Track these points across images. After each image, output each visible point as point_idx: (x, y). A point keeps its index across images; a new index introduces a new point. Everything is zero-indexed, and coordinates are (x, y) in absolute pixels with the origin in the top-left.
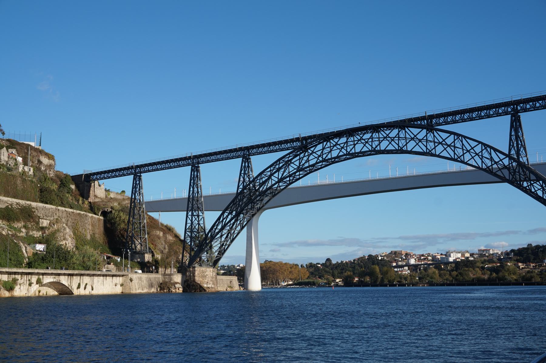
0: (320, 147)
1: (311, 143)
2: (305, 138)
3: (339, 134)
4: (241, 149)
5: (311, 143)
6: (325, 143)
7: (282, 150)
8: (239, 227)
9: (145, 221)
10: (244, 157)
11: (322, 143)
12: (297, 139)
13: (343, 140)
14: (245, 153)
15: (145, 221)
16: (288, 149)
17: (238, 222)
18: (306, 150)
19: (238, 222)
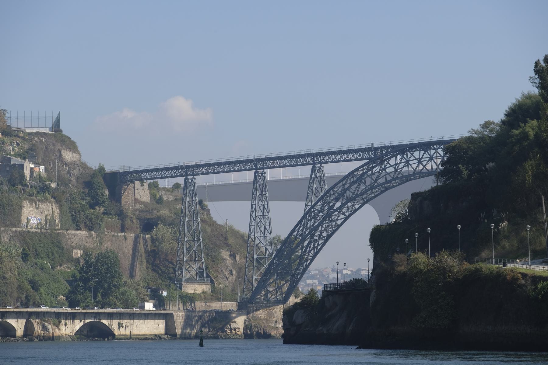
0: (392, 161)
1: (386, 155)
2: (381, 148)
3: (413, 147)
4: (309, 155)
5: (386, 155)
6: (399, 157)
7: (357, 160)
8: (312, 252)
9: (201, 240)
10: (314, 164)
11: (396, 156)
12: (369, 150)
13: (416, 154)
14: (316, 159)
15: (201, 240)
16: (363, 159)
17: (312, 246)
18: (382, 163)
19: (312, 246)
